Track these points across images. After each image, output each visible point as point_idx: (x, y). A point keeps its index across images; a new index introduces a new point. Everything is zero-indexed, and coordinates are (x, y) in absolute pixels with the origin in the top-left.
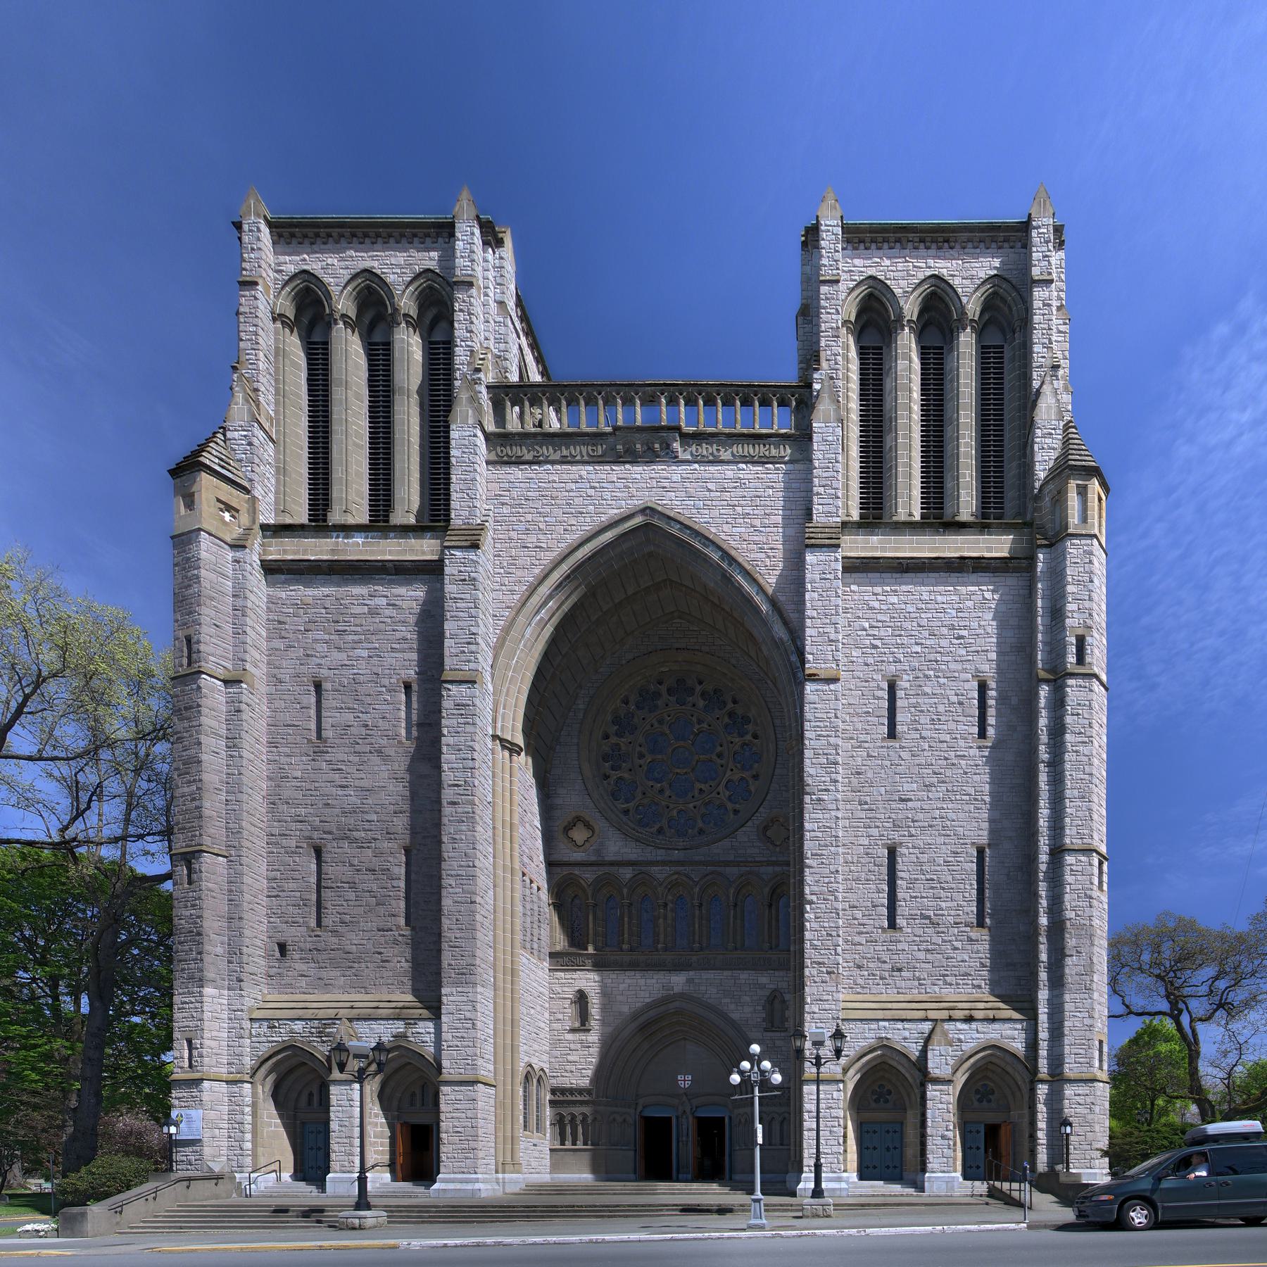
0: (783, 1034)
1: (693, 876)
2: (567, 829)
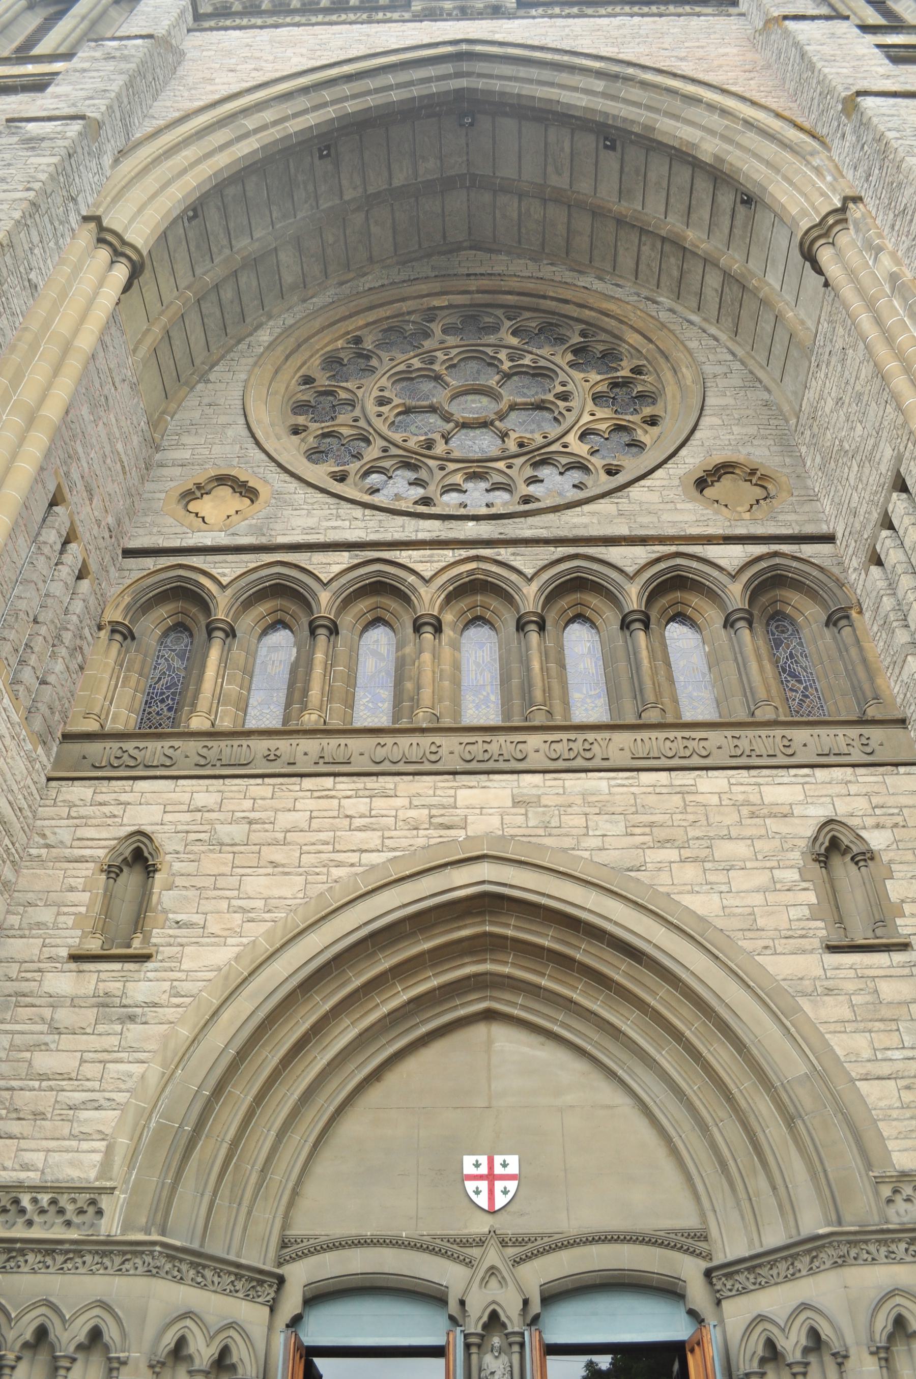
0: (898, 957)
1: (517, 563)
2: (189, 496)
